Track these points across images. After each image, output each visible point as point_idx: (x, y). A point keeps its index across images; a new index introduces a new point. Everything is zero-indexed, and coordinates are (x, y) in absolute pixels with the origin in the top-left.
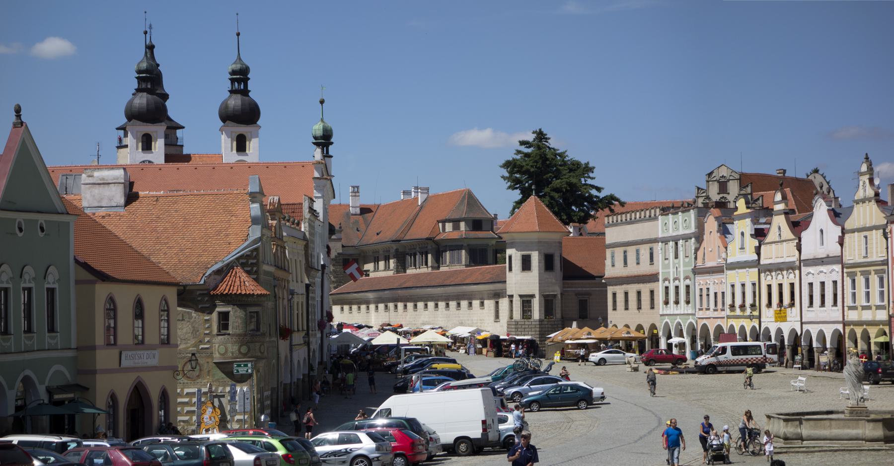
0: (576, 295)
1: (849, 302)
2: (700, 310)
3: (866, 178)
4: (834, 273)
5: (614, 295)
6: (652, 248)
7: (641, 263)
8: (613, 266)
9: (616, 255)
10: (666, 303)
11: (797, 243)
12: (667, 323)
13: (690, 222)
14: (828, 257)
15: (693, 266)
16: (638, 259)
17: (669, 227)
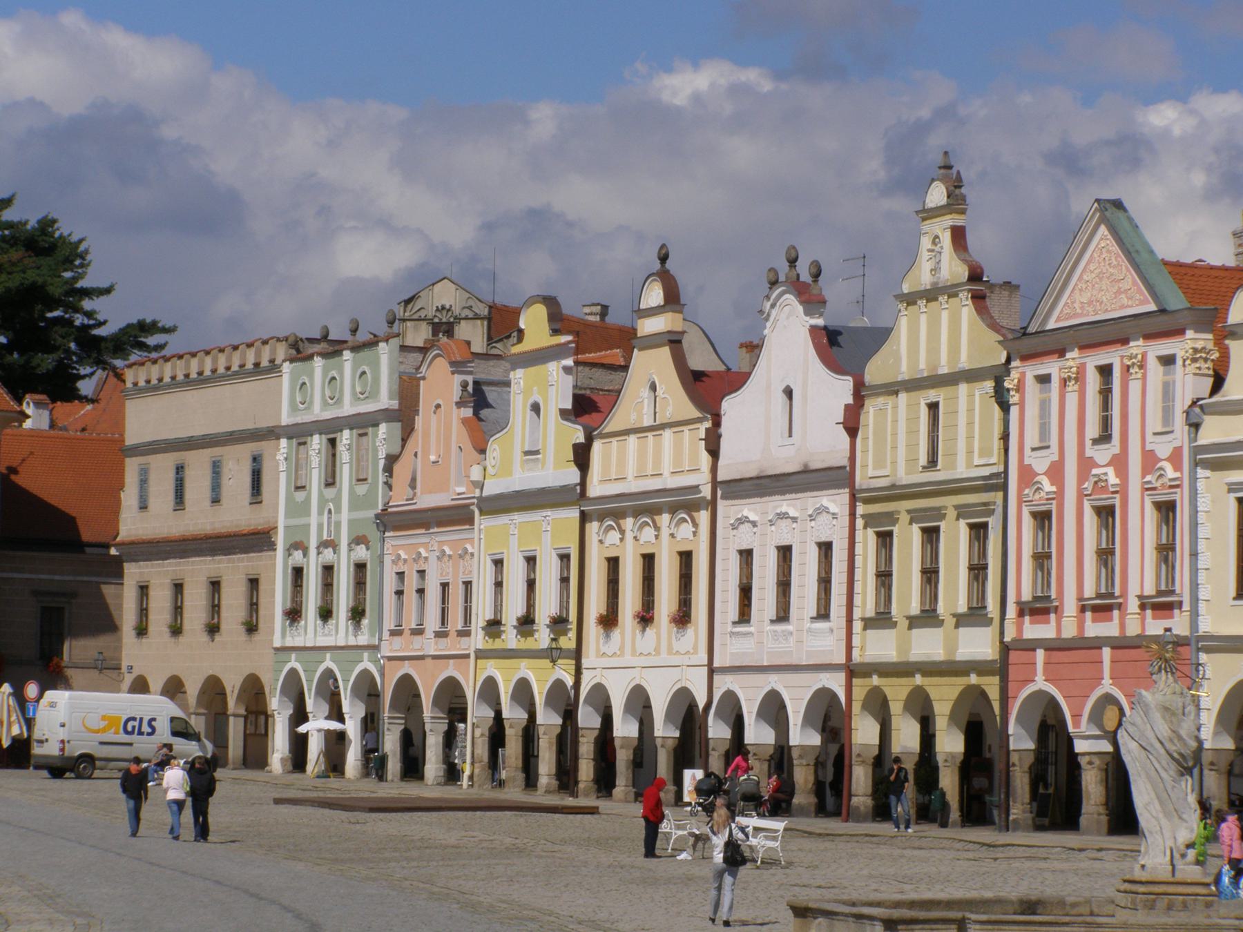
0: (36, 593)
1: (866, 604)
2: (395, 633)
3: (941, 228)
4: (825, 518)
5: (144, 590)
6: (260, 455)
7: (224, 500)
8: (143, 507)
9: (153, 477)
10: (294, 614)
11: (707, 430)
12: (293, 672)
13: (376, 380)
14: (806, 471)
15: (380, 507)
16: (216, 487)
17: (312, 396)
